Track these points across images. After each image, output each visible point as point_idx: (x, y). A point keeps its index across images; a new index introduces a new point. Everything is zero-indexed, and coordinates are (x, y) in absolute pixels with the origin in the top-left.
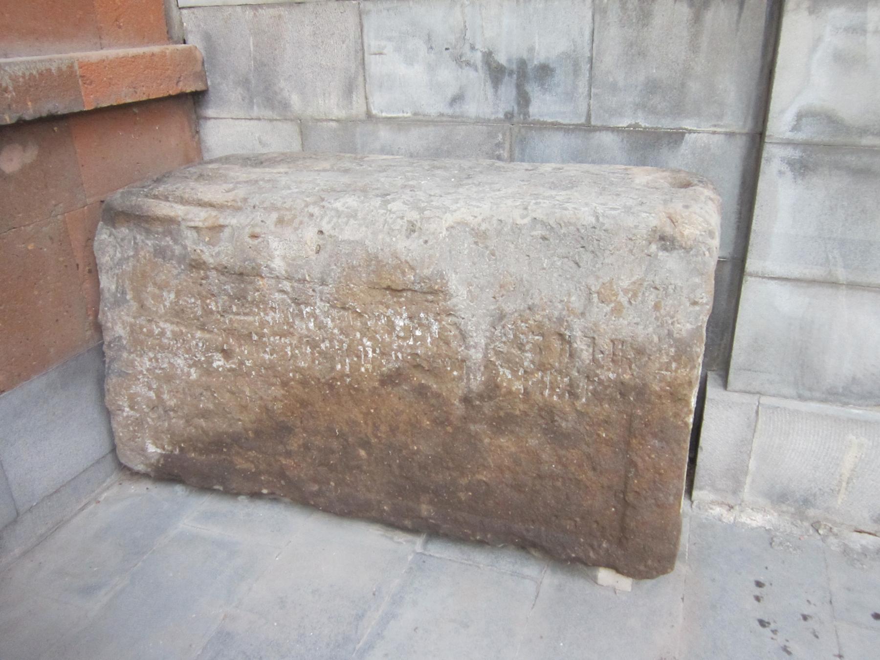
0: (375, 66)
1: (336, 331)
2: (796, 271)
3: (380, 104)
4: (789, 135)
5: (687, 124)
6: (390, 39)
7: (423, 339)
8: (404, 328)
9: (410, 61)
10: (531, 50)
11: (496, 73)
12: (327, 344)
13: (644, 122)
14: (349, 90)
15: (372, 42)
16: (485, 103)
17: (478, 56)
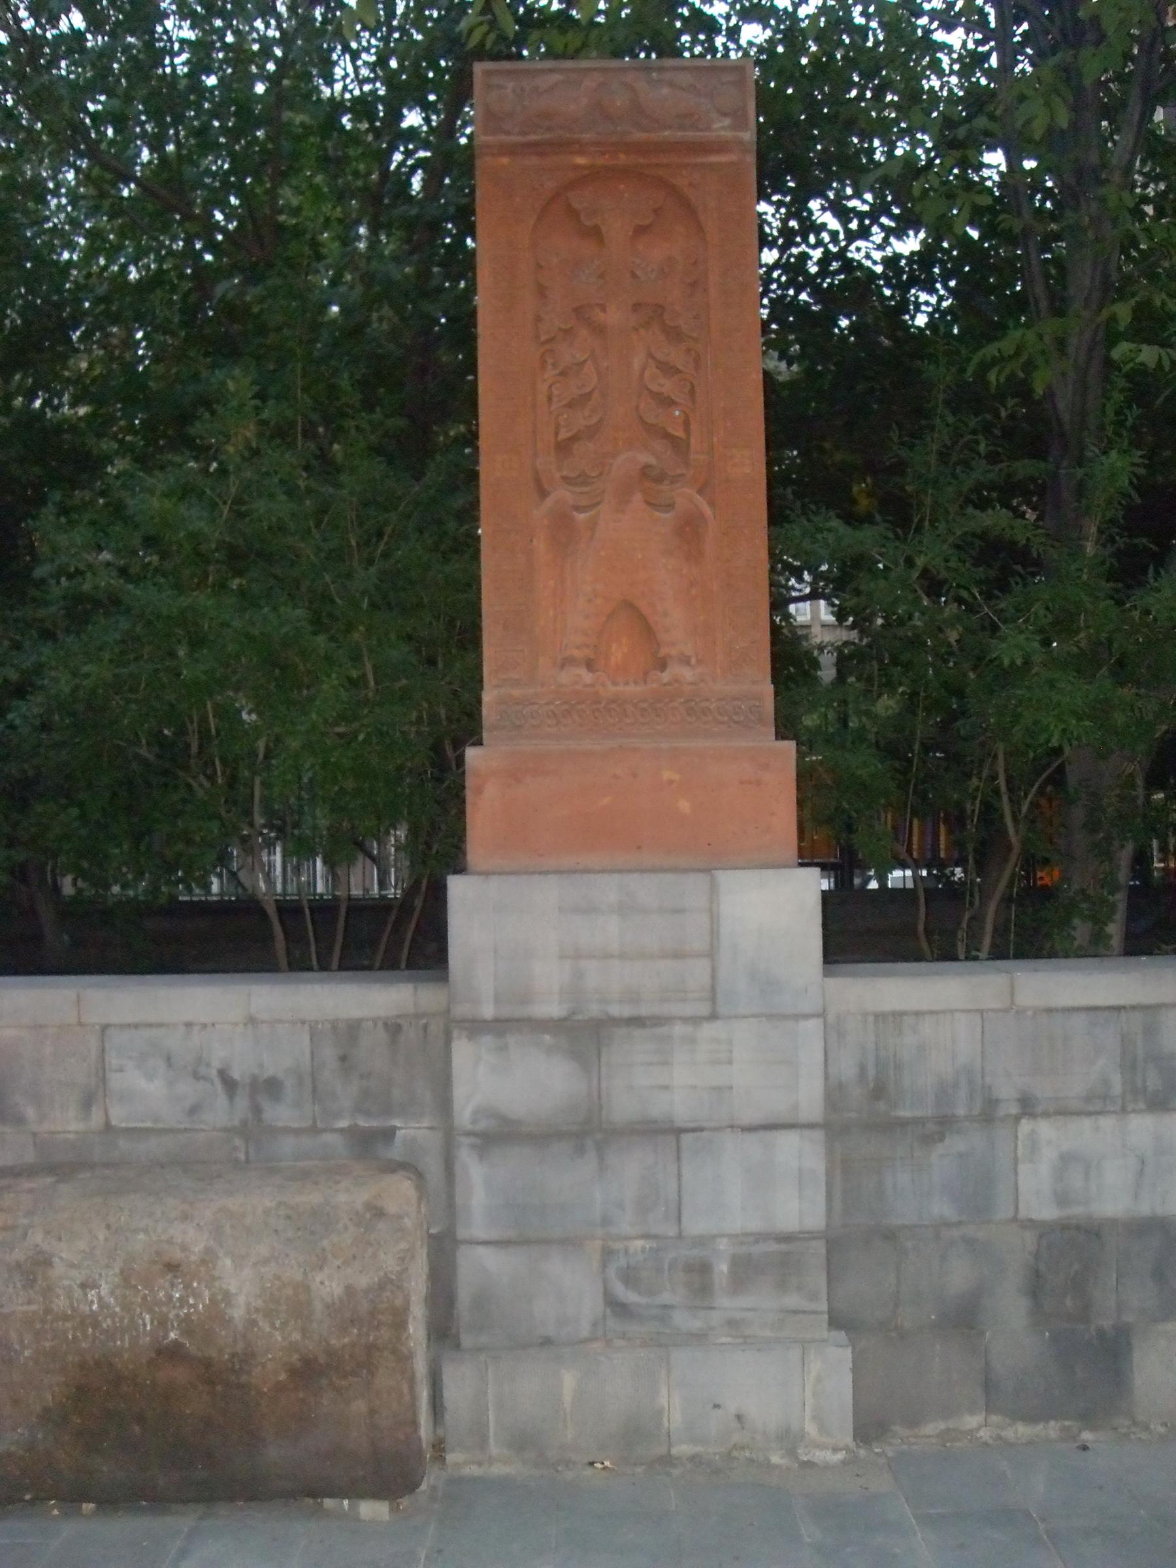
0: (116, 1081)
1: (117, 1309)
2: (494, 1235)
3: (119, 1116)
4: (469, 1127)
5: (397, 1123)
6: (130, 1058)
7: (194, 1306)
8: (180, 1299)
9: (150, 1077)
10: (261, 1066)
11: (230, 1085)
12: (109, 1321)
13: (363, 1123)
14: (87, 1103)
15: (113, 1060)
16: (221, 1113)
17: (214, 1073)
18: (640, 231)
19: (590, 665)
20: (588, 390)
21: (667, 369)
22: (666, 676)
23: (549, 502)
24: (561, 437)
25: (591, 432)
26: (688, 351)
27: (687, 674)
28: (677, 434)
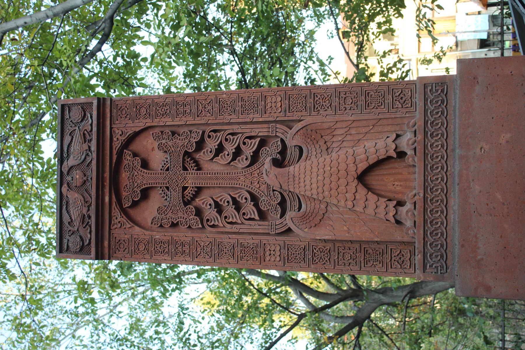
18: (145, 164)
19: (400, 204)
20: (230, 199)
21: (220, 149)
22: (410, 152)
23: (293, 227)
24: (257, 218)
25: (254, 199)
26: (209, 137)
27: (408, 136)
28: (257, 143)
